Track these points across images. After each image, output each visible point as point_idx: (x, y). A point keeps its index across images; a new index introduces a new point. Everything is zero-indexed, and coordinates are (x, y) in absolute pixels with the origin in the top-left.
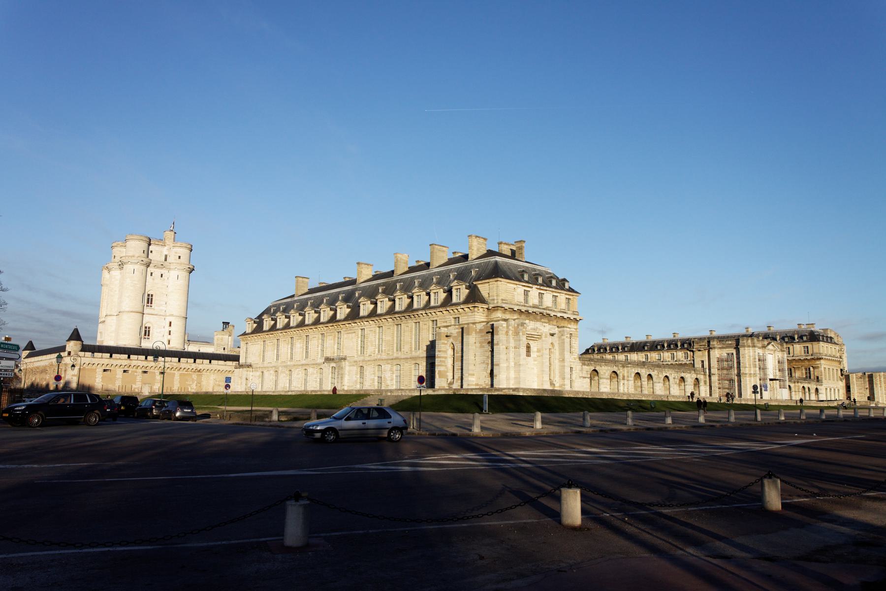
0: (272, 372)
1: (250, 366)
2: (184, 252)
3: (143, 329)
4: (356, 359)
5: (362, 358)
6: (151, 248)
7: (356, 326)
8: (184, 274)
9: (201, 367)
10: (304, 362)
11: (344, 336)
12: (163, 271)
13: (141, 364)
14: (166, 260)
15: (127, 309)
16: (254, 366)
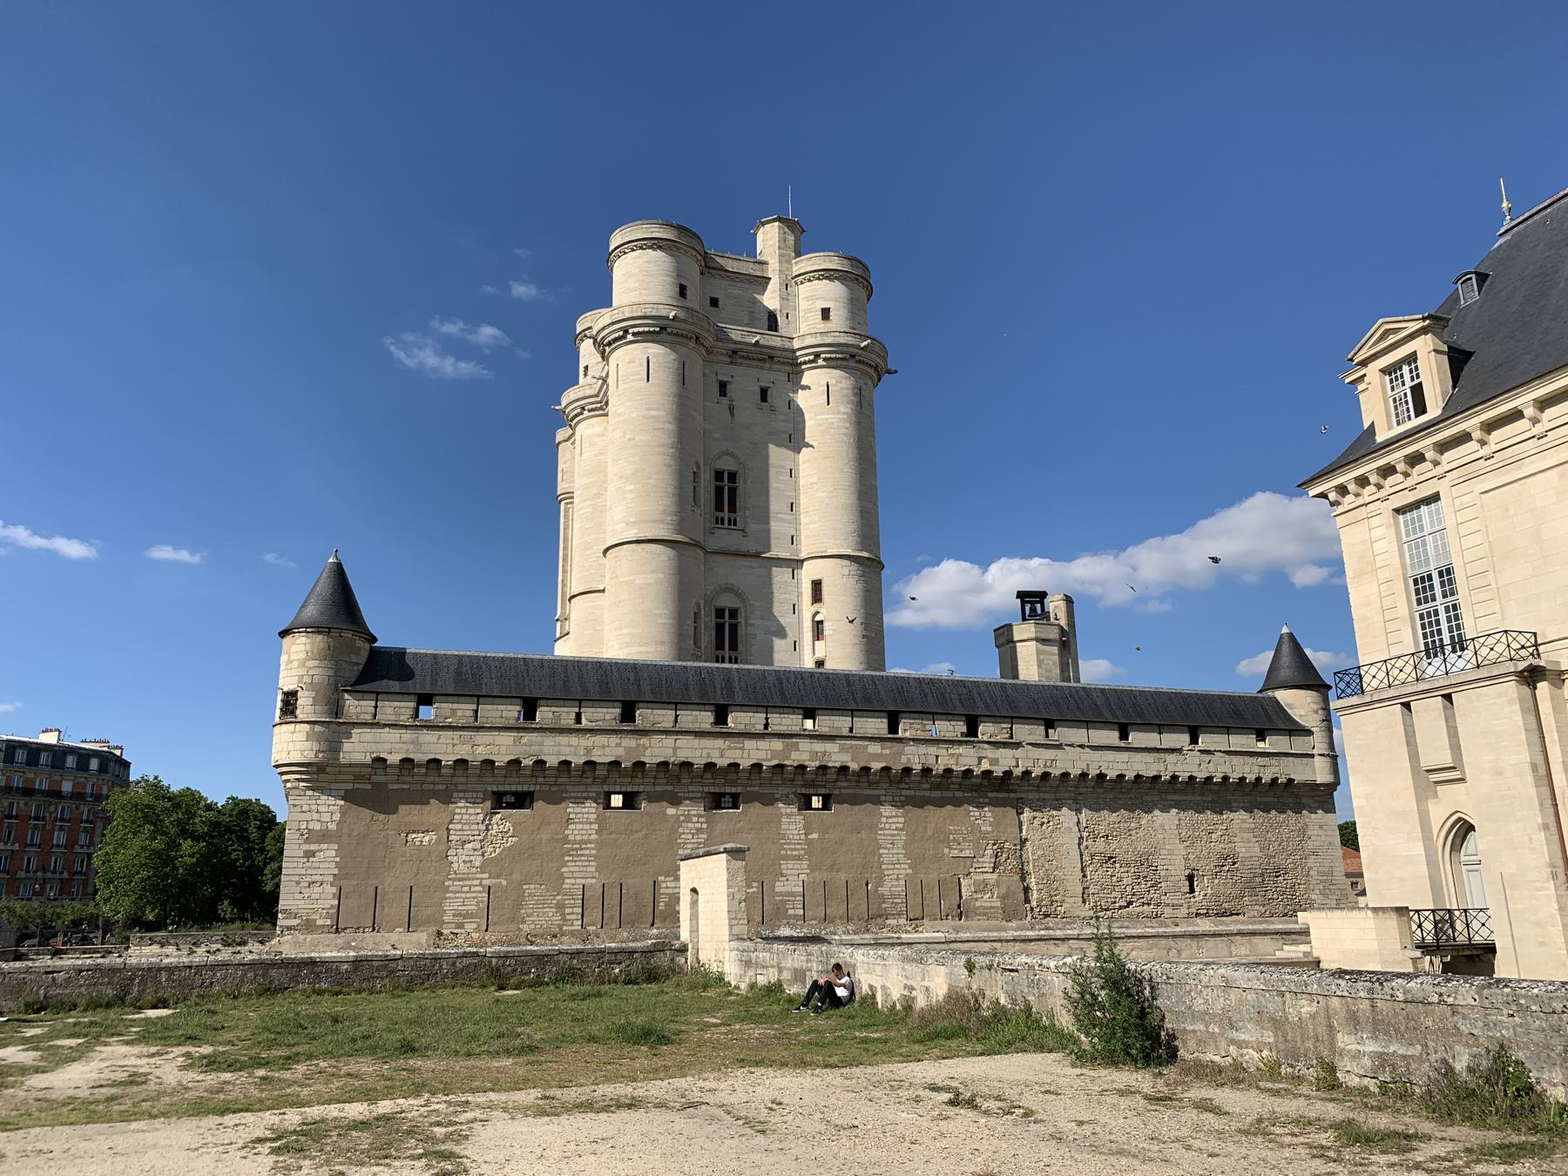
13: (698, 751)
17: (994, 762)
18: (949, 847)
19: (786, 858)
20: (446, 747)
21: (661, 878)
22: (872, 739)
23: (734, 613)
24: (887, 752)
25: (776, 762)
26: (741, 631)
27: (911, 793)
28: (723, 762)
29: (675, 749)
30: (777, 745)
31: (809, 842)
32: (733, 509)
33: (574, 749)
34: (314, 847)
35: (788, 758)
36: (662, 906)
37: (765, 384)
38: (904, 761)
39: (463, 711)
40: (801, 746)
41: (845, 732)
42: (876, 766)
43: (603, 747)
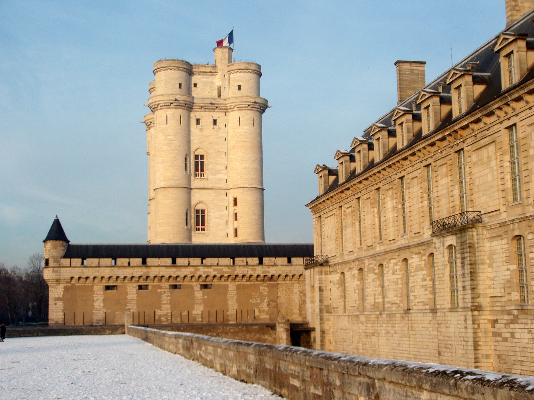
0: (356, 272)
1: (325, 263)
2: (246, 79)
3: (193, 214)
4: (504, 217)
5: (517, 213)
6: (195, 79)
7: (495, 125)
8: (248, 115)
9: (272, 271)
10: (402, 242)
11: (472, 157)
12: (216, 115)
14: (219, 96)
15: (162, 184)
16: (332, 262)
17: (268, 272)
18: (252, 300)
19: (197, 304)
20: (90, 273)
21: (156, 310)
22: (225, 266)
23: (203, 211)
24: (230, 270)
25: (192, 275)
26: (206, 218)
27: (239, 283)
28: (175, 275)
29: (159, 272)
30: (192, 269)
31: (203, 299)
32: (202, 170)
33: (128, 272)
34: (56, 302)
35: (196, 273)
36: (157, 318)
37: (215, 118)
38: (236, 273)
39: (95, 261)
40: (200, 270)
41: (216, 264)
42: (226, 275)
43: (137, 272)
